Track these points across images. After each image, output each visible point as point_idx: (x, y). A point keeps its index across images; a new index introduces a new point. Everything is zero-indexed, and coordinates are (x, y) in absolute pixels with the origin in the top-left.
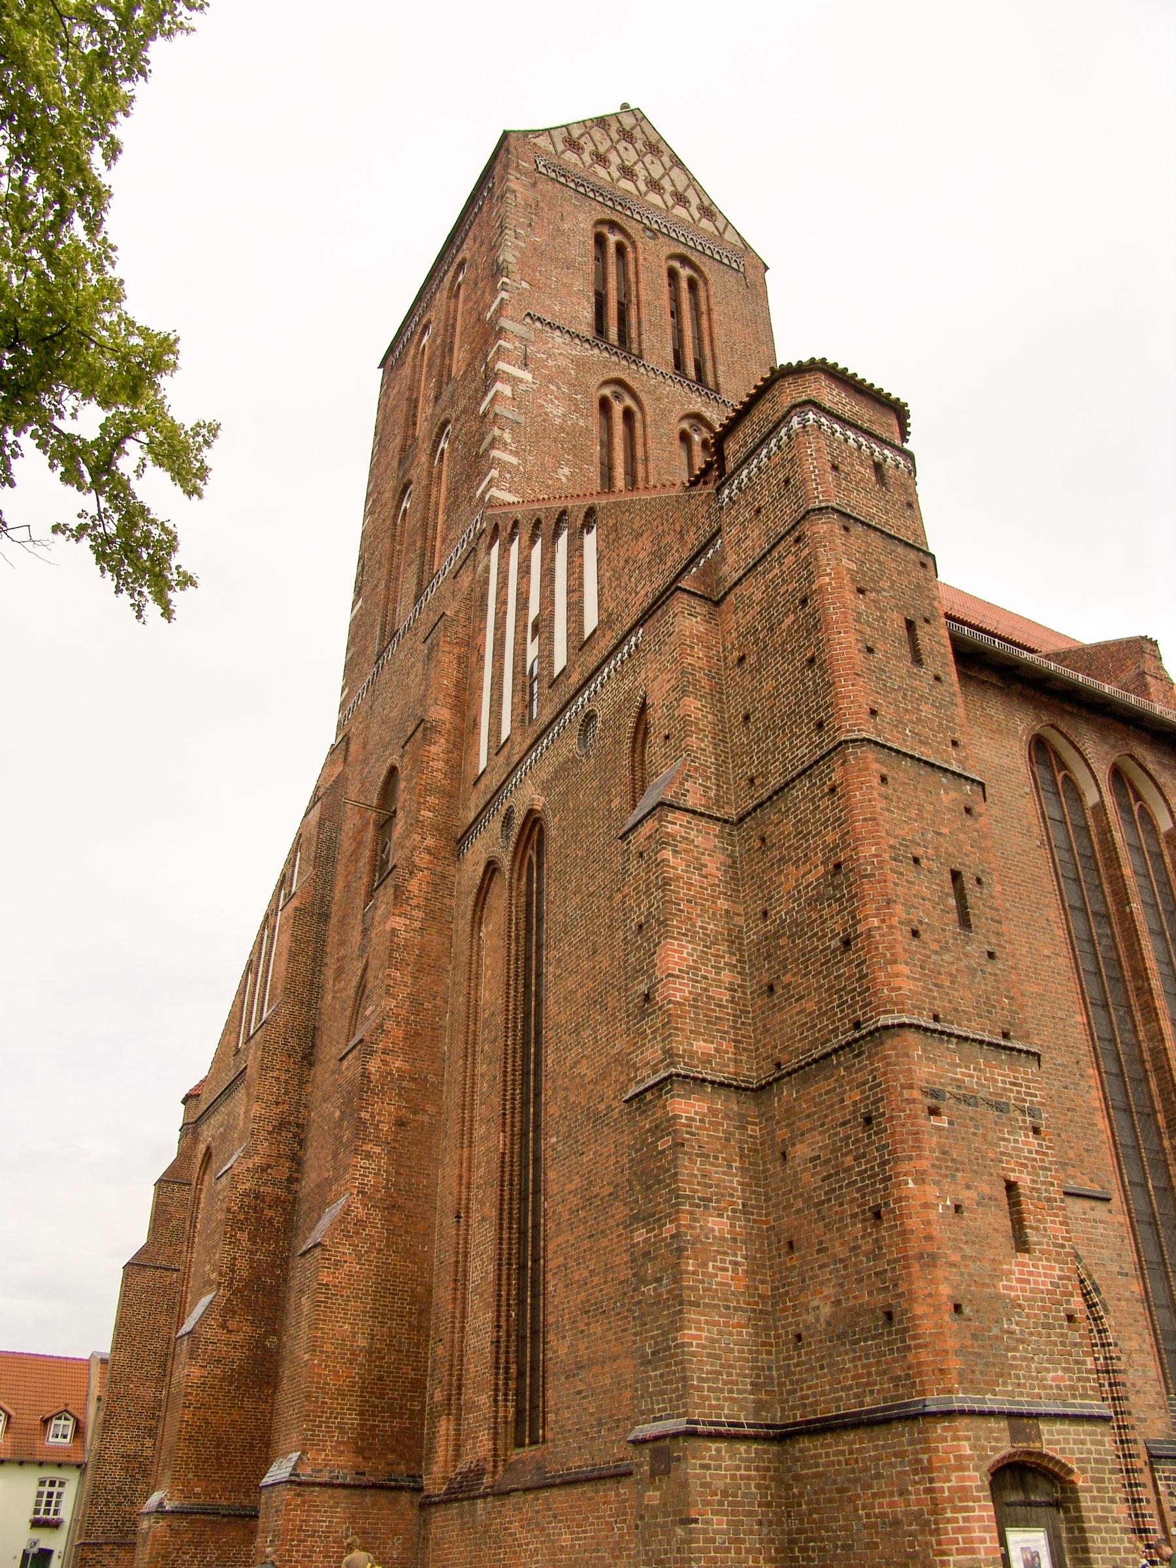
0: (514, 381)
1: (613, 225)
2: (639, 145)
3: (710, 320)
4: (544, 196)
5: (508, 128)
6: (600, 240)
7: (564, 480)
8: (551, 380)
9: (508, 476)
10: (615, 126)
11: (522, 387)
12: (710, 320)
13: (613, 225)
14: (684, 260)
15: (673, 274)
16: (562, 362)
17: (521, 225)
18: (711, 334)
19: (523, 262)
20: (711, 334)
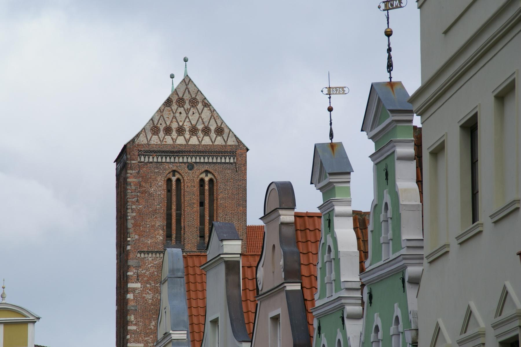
0: (134, 290)
2: (187, 106)
3: (217, 204)
4: (143, 177)
5: (125, 143)
7: (153, 328)
8: (147, 282)
9: (133, 336)
11: (137, 292)
12: (217, 204)
13: (174, 172)
14: (207, 172)
15: (202, 181)
16: (152, 270)
17: (133, 203)
18: (217, 213)
19: (135, 225)
20: (217, 213)
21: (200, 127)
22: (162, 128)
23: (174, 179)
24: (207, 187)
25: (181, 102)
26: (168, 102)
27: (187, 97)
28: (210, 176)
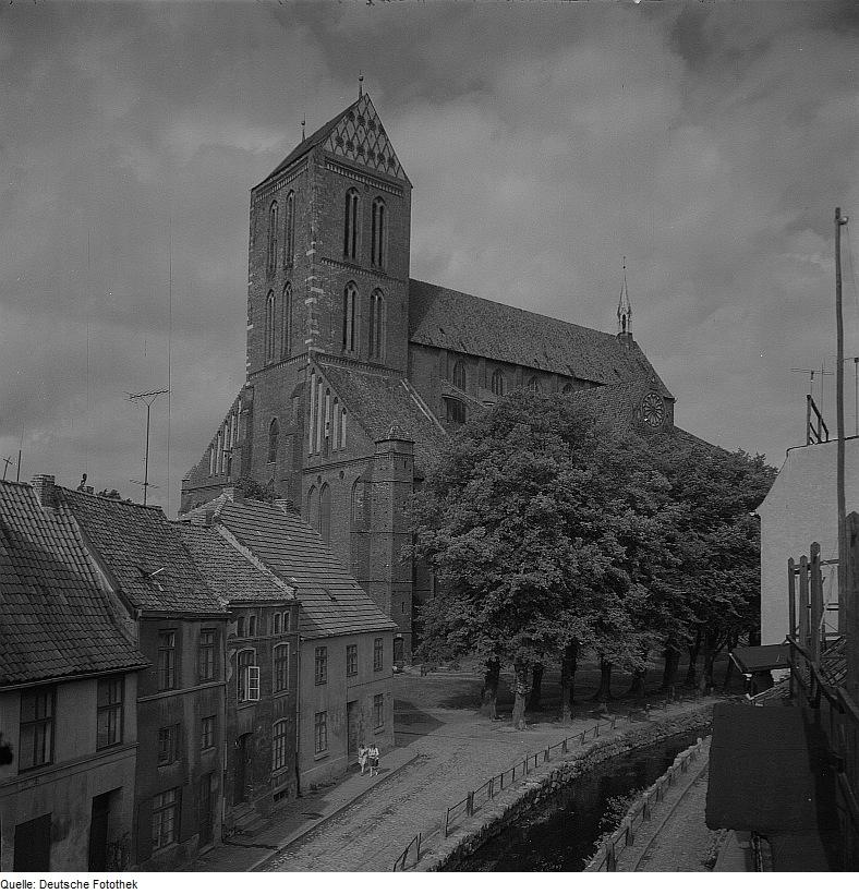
1: (353, 189)
2: (367, 126)
6: (348, 197)
13: (353, 189)
14: (379, 198)
21: (376, 152)
22: (345, 141)
23: (353, 196)
24: (378, 213)
25: (361, 119)
27: (366, 117)
28: (381, 204)
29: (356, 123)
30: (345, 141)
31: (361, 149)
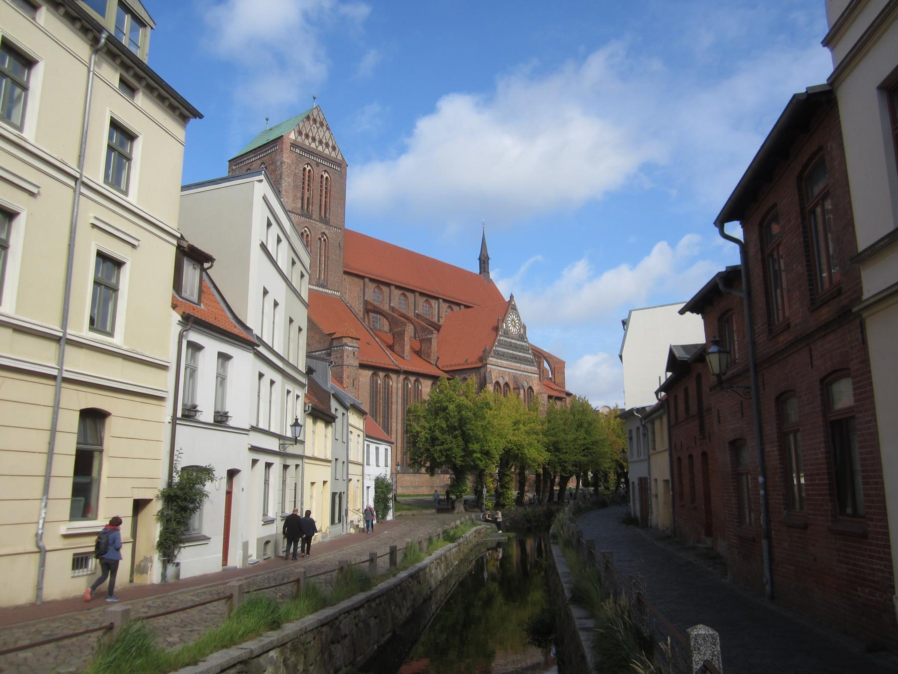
2: (318, 125)
10: (312, 118)
15: (322, 176)
21: (324, 141)
25: (315, 121)
26: (308, 118)
27: (318, 119)
29: (311, 122)
30: (304, 133)
31: (314, 139)
